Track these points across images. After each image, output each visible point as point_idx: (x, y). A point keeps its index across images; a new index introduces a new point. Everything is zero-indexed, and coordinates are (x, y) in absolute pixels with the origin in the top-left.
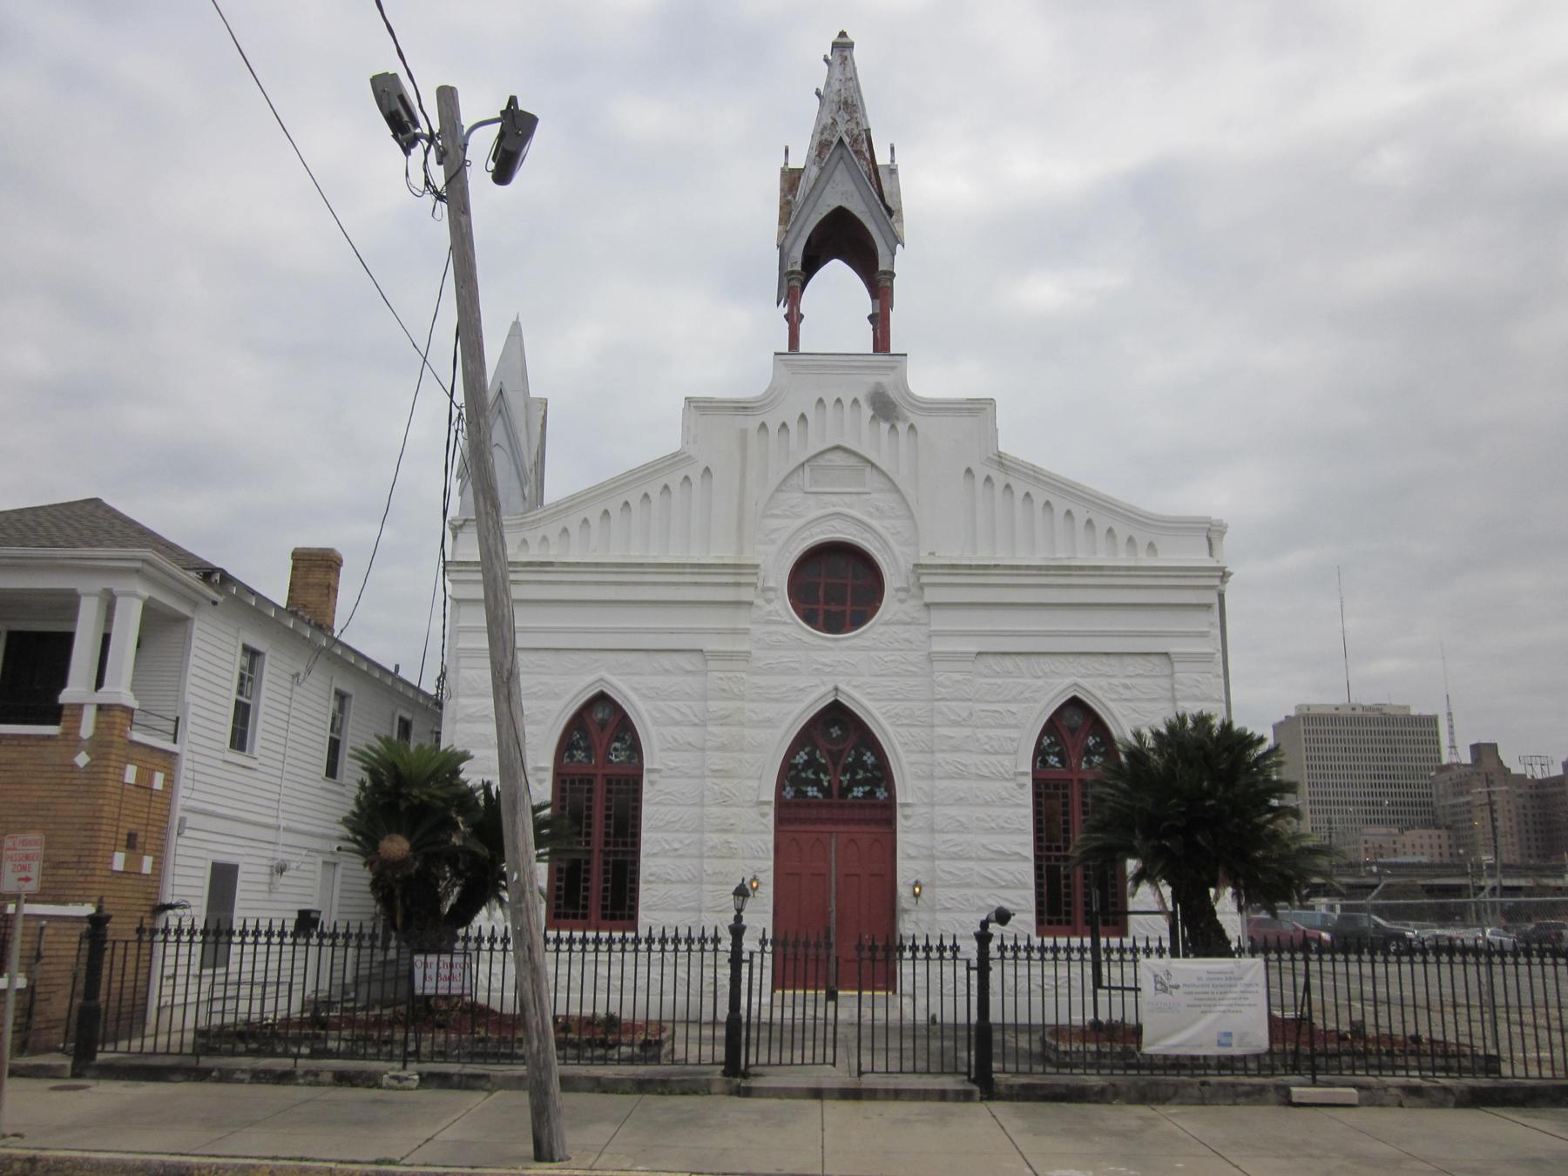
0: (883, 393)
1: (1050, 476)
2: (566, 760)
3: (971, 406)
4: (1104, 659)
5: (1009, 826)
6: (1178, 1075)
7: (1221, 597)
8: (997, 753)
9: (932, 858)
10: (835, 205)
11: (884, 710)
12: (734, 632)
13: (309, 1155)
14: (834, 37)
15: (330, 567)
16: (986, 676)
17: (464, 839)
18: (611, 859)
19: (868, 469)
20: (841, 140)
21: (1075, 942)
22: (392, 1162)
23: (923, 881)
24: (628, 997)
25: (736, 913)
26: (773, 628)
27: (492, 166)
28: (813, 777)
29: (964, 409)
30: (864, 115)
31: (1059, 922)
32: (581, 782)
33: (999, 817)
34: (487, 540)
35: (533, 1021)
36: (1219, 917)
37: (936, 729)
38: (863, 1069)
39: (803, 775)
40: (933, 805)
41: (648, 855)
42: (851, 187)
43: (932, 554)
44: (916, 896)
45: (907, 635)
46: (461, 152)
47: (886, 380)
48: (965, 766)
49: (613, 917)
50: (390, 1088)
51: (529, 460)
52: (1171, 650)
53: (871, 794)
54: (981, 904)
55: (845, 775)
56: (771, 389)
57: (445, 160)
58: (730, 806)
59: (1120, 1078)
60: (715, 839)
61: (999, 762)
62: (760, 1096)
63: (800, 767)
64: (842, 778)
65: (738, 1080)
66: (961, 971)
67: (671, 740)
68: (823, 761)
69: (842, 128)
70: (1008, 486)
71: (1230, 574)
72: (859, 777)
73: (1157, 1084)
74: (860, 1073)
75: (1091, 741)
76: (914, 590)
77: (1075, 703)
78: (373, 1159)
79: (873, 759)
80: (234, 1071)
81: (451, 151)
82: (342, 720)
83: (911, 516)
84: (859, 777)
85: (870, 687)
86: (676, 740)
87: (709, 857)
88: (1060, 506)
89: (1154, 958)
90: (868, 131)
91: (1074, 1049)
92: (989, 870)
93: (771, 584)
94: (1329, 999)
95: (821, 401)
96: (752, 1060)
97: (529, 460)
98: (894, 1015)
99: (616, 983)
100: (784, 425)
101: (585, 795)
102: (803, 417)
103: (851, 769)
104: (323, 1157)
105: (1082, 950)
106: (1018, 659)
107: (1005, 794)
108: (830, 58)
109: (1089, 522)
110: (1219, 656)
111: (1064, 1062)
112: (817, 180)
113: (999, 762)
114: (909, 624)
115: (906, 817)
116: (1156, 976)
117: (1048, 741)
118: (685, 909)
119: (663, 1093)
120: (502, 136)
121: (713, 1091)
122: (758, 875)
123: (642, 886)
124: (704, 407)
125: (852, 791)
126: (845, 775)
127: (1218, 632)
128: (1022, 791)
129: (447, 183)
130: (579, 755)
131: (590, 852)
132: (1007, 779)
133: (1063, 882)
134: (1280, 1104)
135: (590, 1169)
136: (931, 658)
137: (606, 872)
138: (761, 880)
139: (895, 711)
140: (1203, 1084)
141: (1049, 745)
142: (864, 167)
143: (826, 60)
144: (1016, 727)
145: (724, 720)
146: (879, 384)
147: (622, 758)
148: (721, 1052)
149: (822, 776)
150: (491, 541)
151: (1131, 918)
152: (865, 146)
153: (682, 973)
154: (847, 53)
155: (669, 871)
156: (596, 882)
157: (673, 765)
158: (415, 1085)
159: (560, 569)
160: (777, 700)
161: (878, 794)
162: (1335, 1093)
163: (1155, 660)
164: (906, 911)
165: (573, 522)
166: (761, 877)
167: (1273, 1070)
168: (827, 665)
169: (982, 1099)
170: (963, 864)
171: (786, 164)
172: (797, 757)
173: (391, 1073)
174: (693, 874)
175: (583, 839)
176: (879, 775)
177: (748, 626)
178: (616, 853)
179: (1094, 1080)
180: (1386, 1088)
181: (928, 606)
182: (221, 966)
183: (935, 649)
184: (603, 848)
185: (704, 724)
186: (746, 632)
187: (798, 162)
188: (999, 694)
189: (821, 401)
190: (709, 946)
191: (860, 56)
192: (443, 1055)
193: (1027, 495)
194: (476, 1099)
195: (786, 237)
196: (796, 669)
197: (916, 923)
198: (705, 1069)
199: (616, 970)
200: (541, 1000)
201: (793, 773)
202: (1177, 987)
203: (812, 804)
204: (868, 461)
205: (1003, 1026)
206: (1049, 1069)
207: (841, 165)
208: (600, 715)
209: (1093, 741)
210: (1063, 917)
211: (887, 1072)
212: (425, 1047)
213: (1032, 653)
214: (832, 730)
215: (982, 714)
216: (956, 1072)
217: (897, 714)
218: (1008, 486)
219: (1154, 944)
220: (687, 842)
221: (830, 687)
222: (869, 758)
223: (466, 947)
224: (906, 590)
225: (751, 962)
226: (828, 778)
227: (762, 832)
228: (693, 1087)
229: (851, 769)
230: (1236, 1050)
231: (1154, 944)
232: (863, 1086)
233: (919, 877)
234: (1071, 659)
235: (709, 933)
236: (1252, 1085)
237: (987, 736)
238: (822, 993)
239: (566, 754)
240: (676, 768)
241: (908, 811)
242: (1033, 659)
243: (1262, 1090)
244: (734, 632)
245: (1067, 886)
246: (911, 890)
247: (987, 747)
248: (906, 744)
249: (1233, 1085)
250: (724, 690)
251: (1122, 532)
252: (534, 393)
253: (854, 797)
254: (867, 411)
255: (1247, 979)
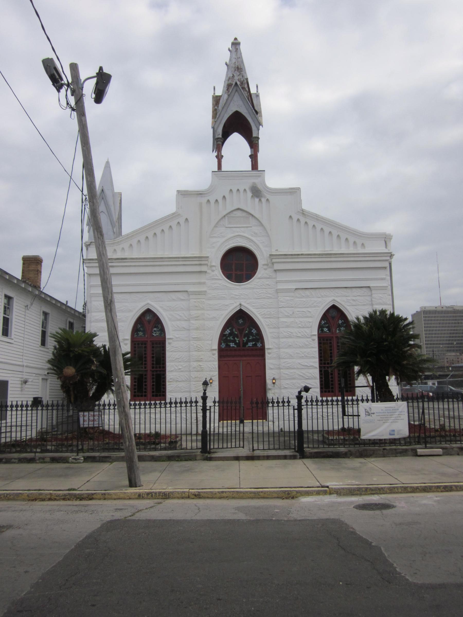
0: (256, 186)
1: (322, 218)
2: (135, 336)
3: (291, 191)
4: (345, 290)
5: (309, 355)
6: (375, 446)
7: (390, 264)
8: (304, 327)
9: (280, 369)
10: (234, 109)
11: (259, 312)
12: (200, 283)
13: (42, 489)
14: (232, 40)
15: (38, 263)
16: (299, 298)
17: (97, 367)
18: (155, 373)
19: (251, 217)
20: (236, 83)
21: (335, 398)
22: (74, 490)
23: (276, 378)
24: (163, 426)
25: (203, 391)
26: (214, 281)
27: (94, 96)
28: (232, 339)
29: (289, 192)
30: (245, 73)
31: (329, 392)
32: (142, 344)
33: (305, 352)
34: (99, 249)
35: (126, 435)
36: (390, 387)
37: (280, 319)
38: (255, 448)
39: (229, 338)
40: (279, 348)
41: (169, 371)
42: (241, 103)
43: (277, 250)
44: (274, 383)
45: (267, 283)
46: (81, 90)
47: (257, 181)
48: (292, 333)
49: (156, 396)
50: (72, 463)
51: (115, 217)
52: (371, 285)
53: (255, 345)
54: (299, 386)
55: (245, 338)
56: (211, 186)
57: (74, 94)
58: (201, 351)
59: (352, 449)
60: (195, 364)
61: (305, 331)
62: (215, 460)
63: (227, 335)
64: (244, 339)
65: (207, 454)
66: (291, 411)
67: (176, 327)
68: (236, 333)
69: (236, 78)
70: (306, 223)
71: (394, 255)
72: (250, 338)
73: (366, 450)
74: (253, 450)
75: (340, 322)
76: (270, 265)
77: (334, 308)
78: (67, 489)
79: (255, 331)
80: (11, 459)
81: (77, 91)
82: (46, 323)
83: (268, 236)
84: (250, 338)
85: (254, 303)
86: (178, 326)
87: (193, 371)
88: (327, 230)
89: (365, 403)
90: (247, 79)
91: (335, 438)
92: (302, 373)
93: (213, 264)
94: (432, 417)
95: (231, 190)
96: (212, 447)
97: (115, 217)
98: (266, 429)
99: (158, 420)
100: (217, 201)
101: (144, 349)
102: (224, 197)
103: (247, 335)
104: (48, 489)
105: (337, 401)
106: (311, 291)
107: (307, 343)
108: (231, 49)
109: (338, 236)
110: (390, 287)
111: (331, 443)
112: (227, 100)
113: (305, 331)
114: (269, 278)
115: (269, 353)
116: (366, 410)
117: (324, 322)
118: (184, 392)
119: (178, 461)
120: (97, 84)
121: (197, 459)
122: (213, 378)
123: (167, 383)
124: (184, 194)
125: (248, 344)
126: (245, 338)
127: (389, 278)
128: (314, 342)
129: (76, 103)
130: (141, 334)
131: (146, 371)
132: (308, 338)
133: (330, 376)
134: (413, 456)
135: (151, 489)
136: (277, 291)
137: (153, 378)
138: (213, 379)
139: (264, 312)
140: (384, 449)
141: (325, 323)
142: (245, 94)
143: (229, 50)
144: (311, 317)
145: (197, 318)
146: (254, 183)
147: (157, 334)
148: (200, 445)
149: (236, 338)
150: (101, 249)
151: (357, 389)
152: (246, 86)
153: (184, 416)
154: (238, 47)
155: (178, 377)
156: (149, 383)
157: (177, 336)
158: (82, 461)
159: (130, 261)
160: (217, 310)
161: (258, 345)
162: (433, 451)
163: (364, 289)
164: (270, 389)
165: (134, 242)
166: (213, 378)
167: (410, 444)
168: (237, 295)
169: (300, 458)
170: (292, 371)
171: (214, 94)
172: (226, 332)
173: (73, 457)
174: (187, 378)
175: (143, 366)
176: (258, 337)
177: (205, 281)
178: (157, 371)
179: (342, 449)
180: (453, 448)
181: (275, 271)
182: (4, 420)
183: (279, 288)
184: (152, 369)
185: (188, 320)
186: (204, 283)
187: (219, 92)
188: (304, 304)
189: (231, 190)
190: (194, 404)
191: (243, 48)
192: (93, 450)
193: (314, 226)
194: (106, 466)
195: (215, 124)
196: (224, 297)
197: (274, 394)
198: (194, 451)
199: (158, 416)
200: (129, 427)
201: (224, 338)
202: (374, 414)
203: (233, 349)
204: (251, 214)
205: (308, 431)
206: (325, 446)
207: (237, 93)
208: (148, 318)
209: (341, 322)
210: (330, 390)
211: (264, 449)
212: (85, 447)
213: (317, 288)
214: (239, 321)
215: (298, 313)
216: (290, 449)
217: (265, 314)
218: (306, 223)
219: (365, 398)
220: (184, 366)
221: (238, 304)
222: (254, 331)
223: (99, 409)
224: (267, 265)
225: (210, 410)
226: (238, 339)
227: (214, 361)
228: (190, 457)
229: (247, 335)
230: (396, 436)
231: (365, 398)
232: (254, 455)
233: (274, 376)
234: (332, 290)
235: (194, 400)
236: (402, 449)
237: (300, 321)
238: (238, 422)
239: (135, 333)
240: (179, 337)
241: (270, 351)
242: (317, 291)
243: (406, 451)
244: (200, 283)
245: (332, 378)
246: (272, 381)
247: (300, 325)
248: (268, 325)
249: (395, 449)
250: (196, 306)
251: (351, 240)
252: (116, 190)
253: (250, 346)
254: (249, 194)
255: (400, 410)
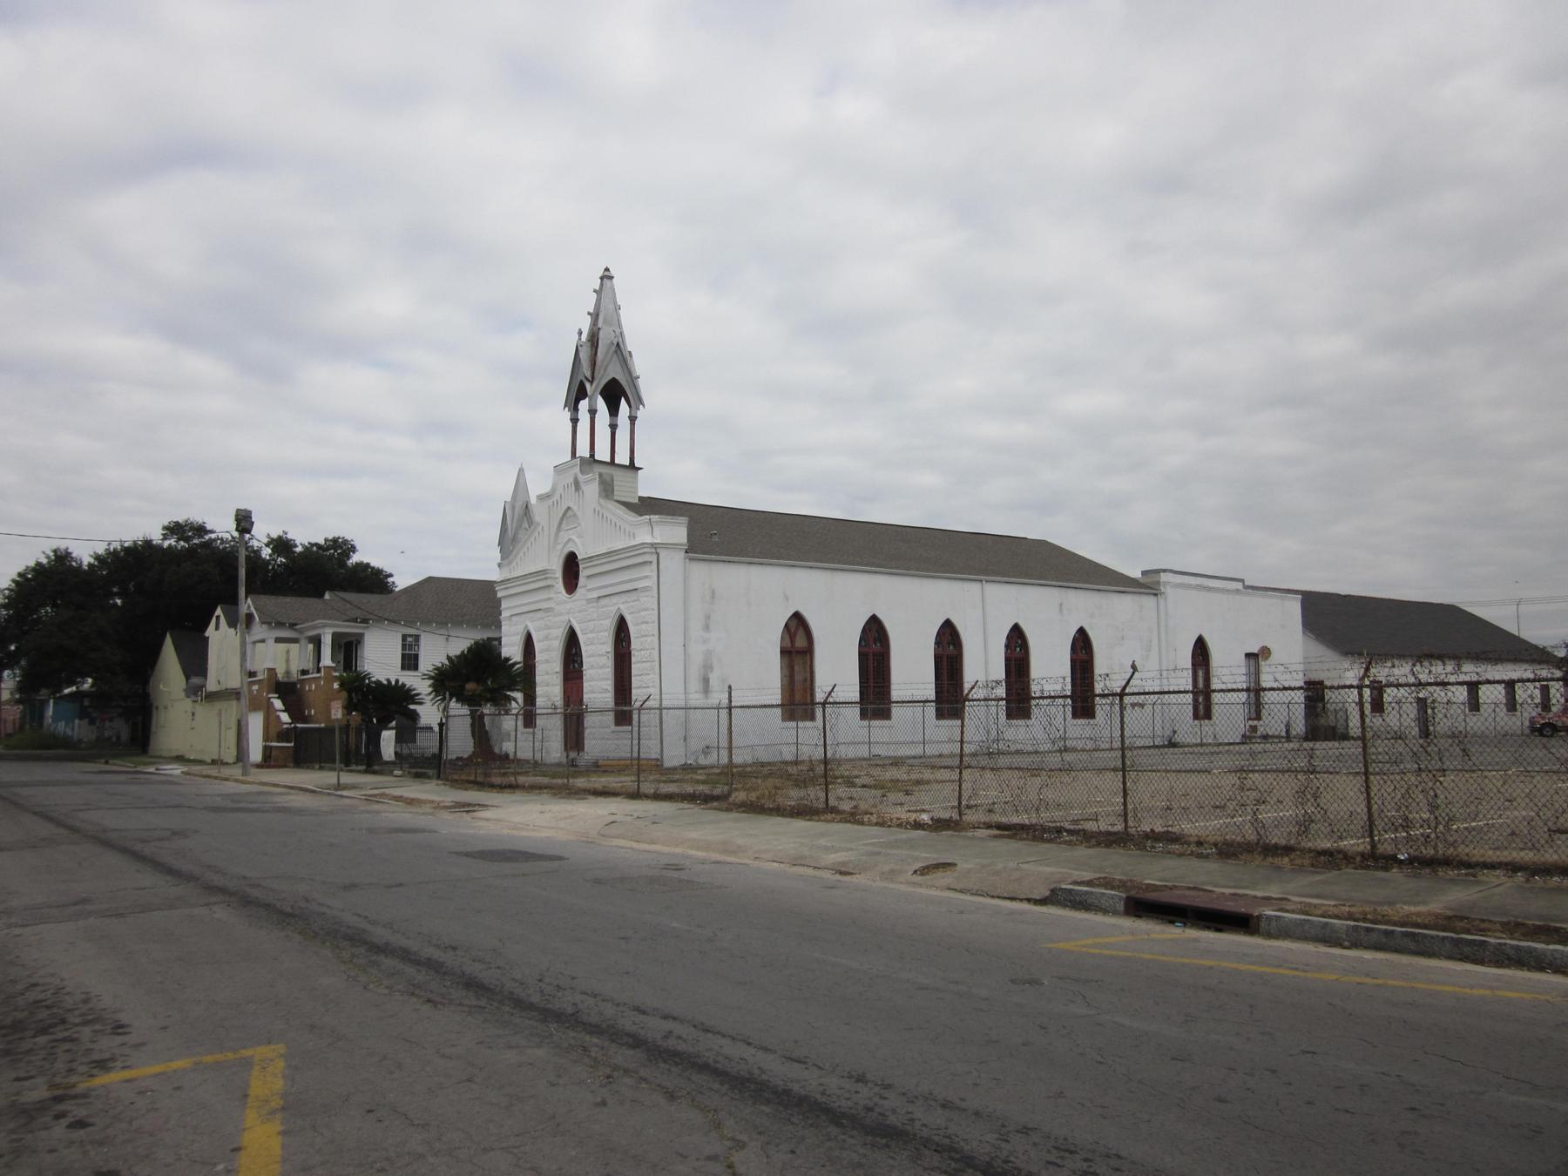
14: (600, 274)
